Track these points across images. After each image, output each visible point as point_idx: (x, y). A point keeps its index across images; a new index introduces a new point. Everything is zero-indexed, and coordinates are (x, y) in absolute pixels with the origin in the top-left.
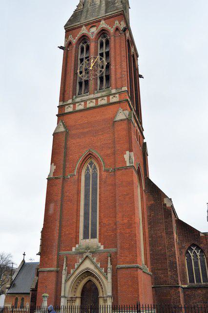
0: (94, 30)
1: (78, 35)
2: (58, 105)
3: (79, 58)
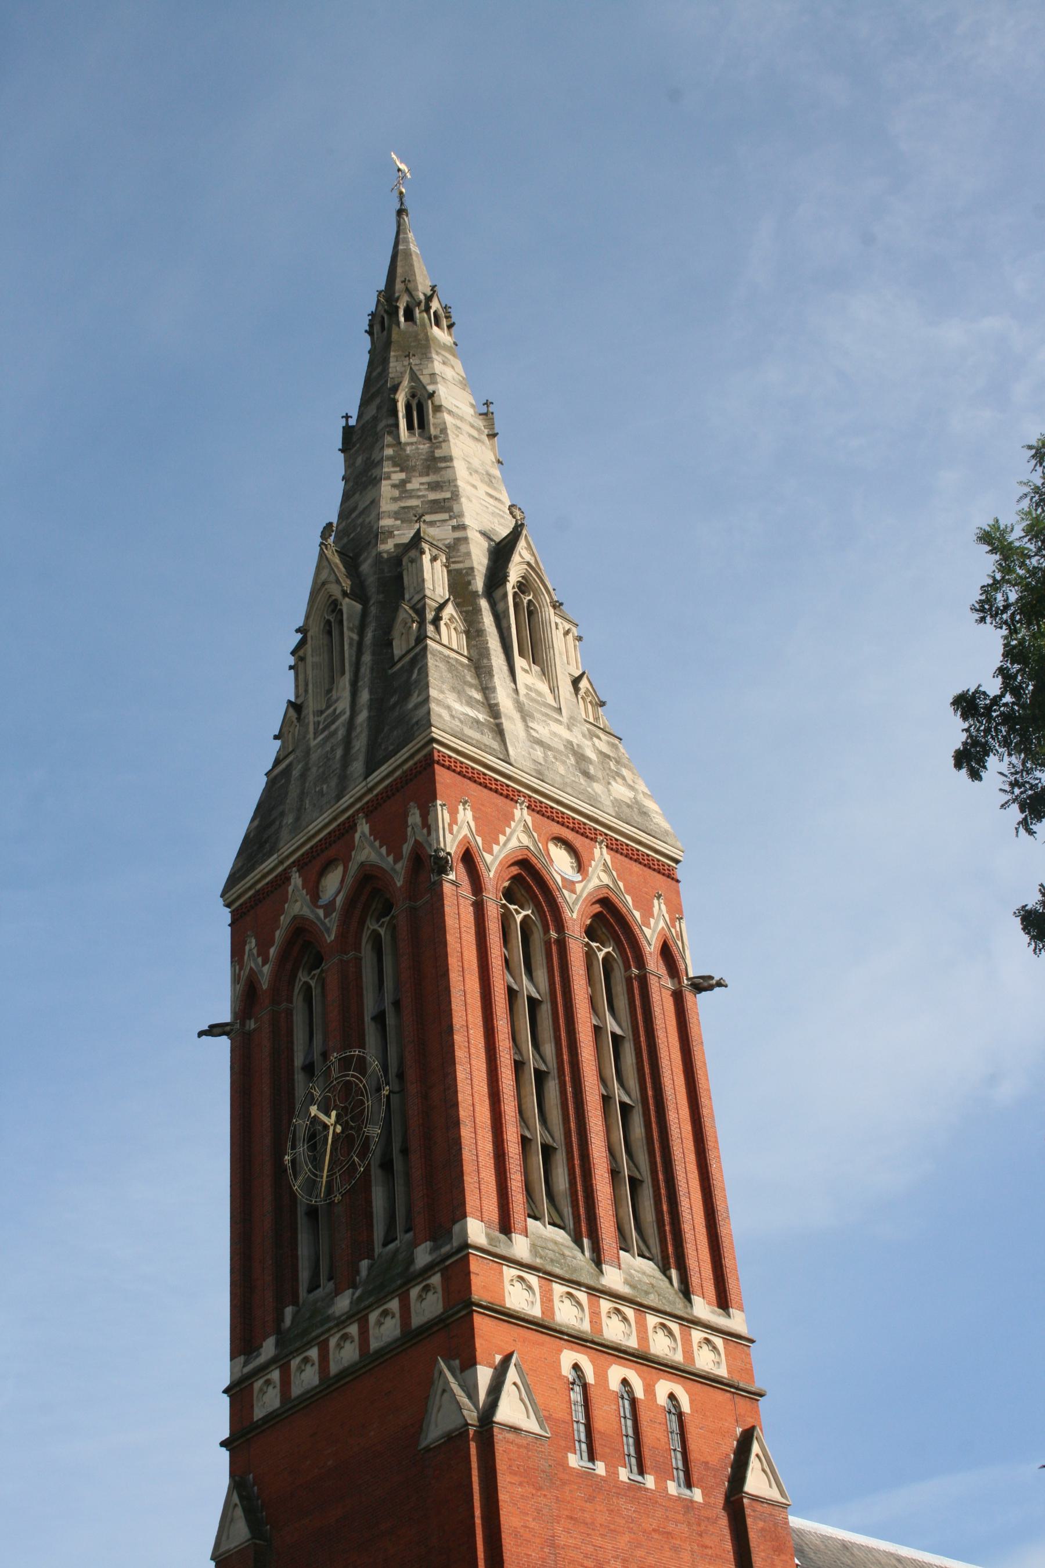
0: (332, 883)
1: (277, 933)
2: (226, 1382)
3: (299, 1061)
